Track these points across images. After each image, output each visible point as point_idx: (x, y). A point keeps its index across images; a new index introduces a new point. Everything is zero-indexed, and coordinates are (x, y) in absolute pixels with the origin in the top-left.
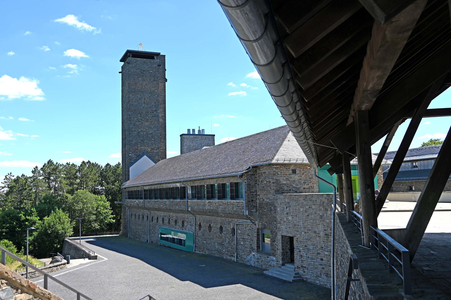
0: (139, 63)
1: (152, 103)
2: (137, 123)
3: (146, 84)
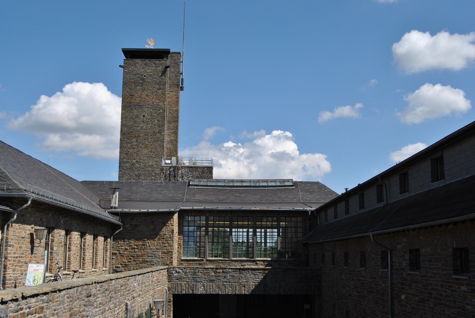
0: (138, 65)
1: (154, 122)
2: (131, 151)
3: (147, 95)
